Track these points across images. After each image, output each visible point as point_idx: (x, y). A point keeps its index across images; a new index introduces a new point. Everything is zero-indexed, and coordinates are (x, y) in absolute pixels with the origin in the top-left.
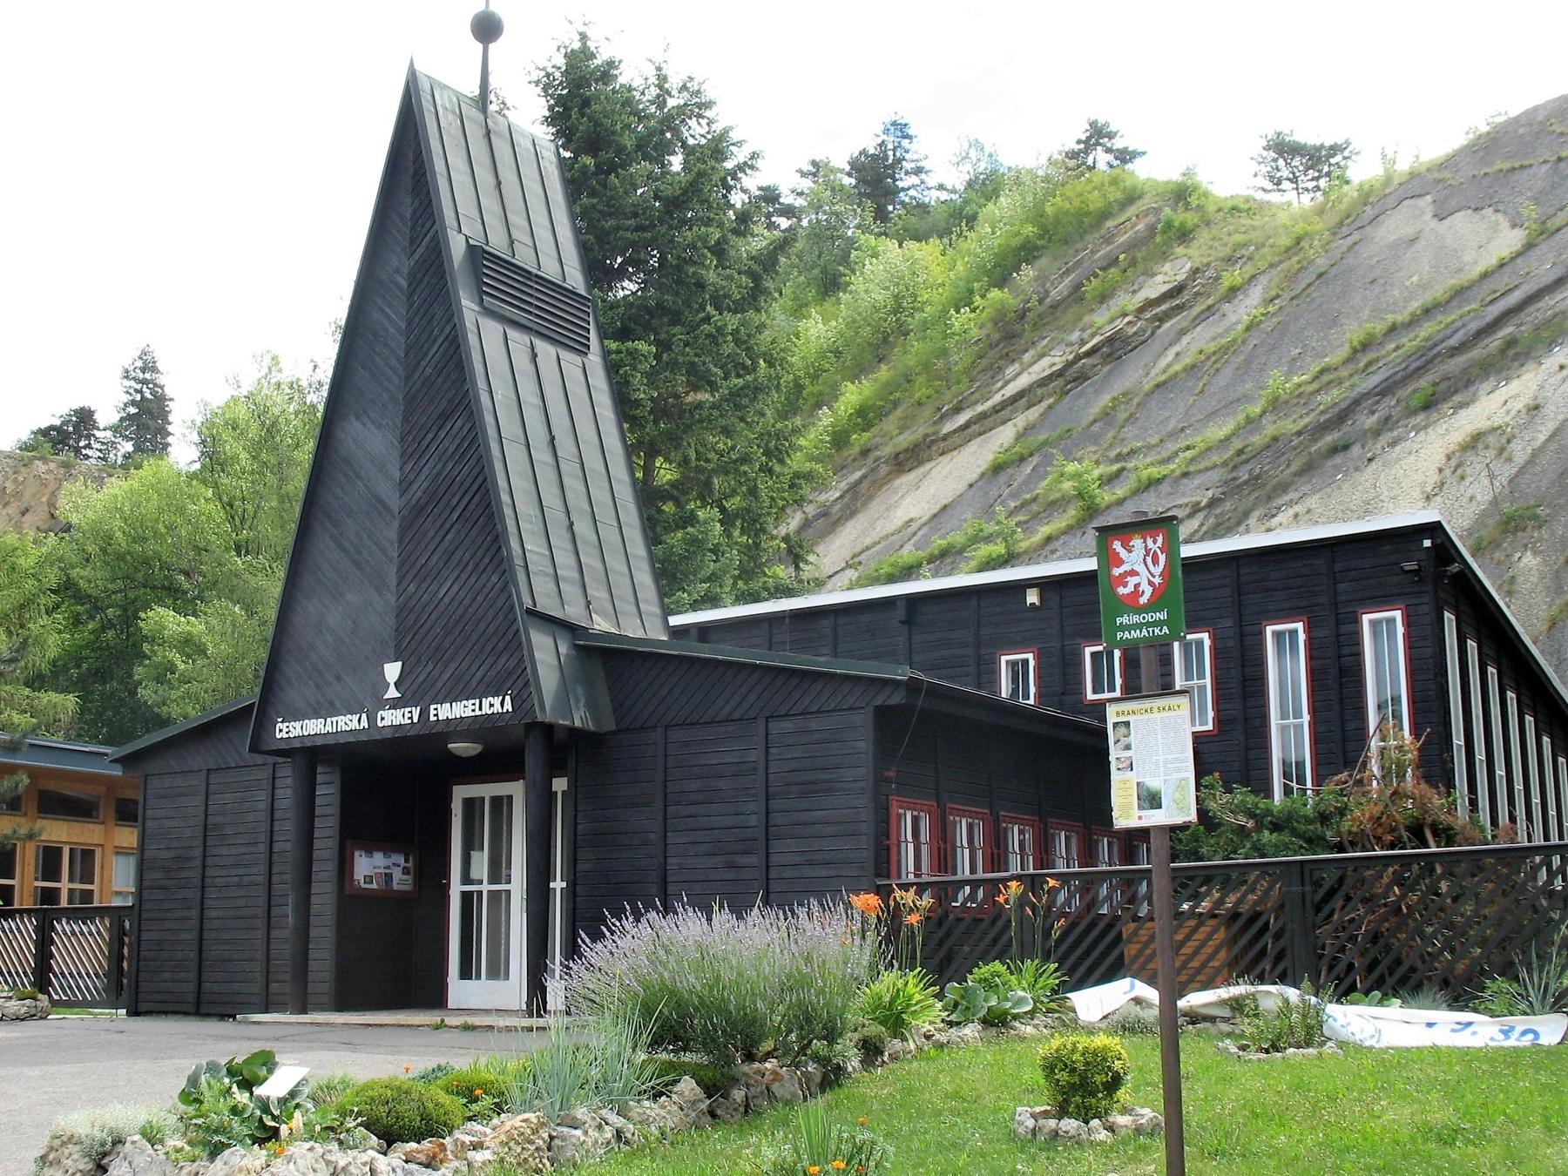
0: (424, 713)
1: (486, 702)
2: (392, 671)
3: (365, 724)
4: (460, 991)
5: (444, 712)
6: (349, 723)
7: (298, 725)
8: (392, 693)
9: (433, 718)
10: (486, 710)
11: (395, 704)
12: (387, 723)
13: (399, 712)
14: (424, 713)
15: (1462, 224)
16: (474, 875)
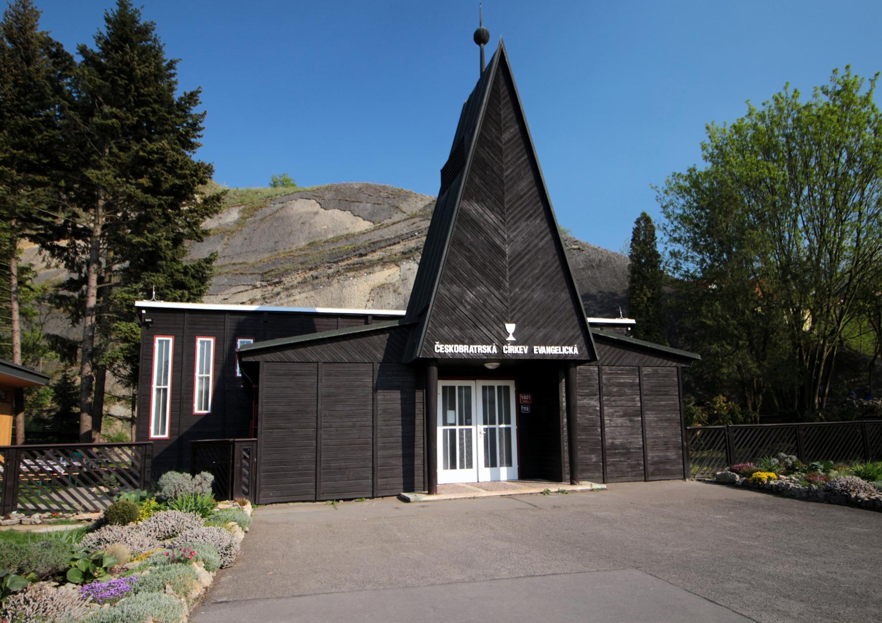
0: (531, 350)
1: (564, 348)
2: (511, 328)
3: (495, 350)
4: (444, 475)
5: (542, 350)
8: (511, 338)
9: (535, 352)
10: (564, 352)
11: (514, 343)
12: (510, 351)
13: (516, 348)
14: (531, 350)
15: (337, 213)
16: (450, 419)
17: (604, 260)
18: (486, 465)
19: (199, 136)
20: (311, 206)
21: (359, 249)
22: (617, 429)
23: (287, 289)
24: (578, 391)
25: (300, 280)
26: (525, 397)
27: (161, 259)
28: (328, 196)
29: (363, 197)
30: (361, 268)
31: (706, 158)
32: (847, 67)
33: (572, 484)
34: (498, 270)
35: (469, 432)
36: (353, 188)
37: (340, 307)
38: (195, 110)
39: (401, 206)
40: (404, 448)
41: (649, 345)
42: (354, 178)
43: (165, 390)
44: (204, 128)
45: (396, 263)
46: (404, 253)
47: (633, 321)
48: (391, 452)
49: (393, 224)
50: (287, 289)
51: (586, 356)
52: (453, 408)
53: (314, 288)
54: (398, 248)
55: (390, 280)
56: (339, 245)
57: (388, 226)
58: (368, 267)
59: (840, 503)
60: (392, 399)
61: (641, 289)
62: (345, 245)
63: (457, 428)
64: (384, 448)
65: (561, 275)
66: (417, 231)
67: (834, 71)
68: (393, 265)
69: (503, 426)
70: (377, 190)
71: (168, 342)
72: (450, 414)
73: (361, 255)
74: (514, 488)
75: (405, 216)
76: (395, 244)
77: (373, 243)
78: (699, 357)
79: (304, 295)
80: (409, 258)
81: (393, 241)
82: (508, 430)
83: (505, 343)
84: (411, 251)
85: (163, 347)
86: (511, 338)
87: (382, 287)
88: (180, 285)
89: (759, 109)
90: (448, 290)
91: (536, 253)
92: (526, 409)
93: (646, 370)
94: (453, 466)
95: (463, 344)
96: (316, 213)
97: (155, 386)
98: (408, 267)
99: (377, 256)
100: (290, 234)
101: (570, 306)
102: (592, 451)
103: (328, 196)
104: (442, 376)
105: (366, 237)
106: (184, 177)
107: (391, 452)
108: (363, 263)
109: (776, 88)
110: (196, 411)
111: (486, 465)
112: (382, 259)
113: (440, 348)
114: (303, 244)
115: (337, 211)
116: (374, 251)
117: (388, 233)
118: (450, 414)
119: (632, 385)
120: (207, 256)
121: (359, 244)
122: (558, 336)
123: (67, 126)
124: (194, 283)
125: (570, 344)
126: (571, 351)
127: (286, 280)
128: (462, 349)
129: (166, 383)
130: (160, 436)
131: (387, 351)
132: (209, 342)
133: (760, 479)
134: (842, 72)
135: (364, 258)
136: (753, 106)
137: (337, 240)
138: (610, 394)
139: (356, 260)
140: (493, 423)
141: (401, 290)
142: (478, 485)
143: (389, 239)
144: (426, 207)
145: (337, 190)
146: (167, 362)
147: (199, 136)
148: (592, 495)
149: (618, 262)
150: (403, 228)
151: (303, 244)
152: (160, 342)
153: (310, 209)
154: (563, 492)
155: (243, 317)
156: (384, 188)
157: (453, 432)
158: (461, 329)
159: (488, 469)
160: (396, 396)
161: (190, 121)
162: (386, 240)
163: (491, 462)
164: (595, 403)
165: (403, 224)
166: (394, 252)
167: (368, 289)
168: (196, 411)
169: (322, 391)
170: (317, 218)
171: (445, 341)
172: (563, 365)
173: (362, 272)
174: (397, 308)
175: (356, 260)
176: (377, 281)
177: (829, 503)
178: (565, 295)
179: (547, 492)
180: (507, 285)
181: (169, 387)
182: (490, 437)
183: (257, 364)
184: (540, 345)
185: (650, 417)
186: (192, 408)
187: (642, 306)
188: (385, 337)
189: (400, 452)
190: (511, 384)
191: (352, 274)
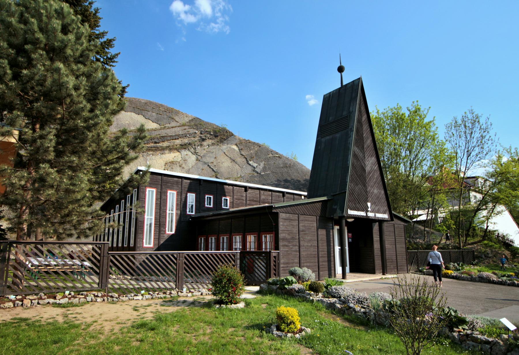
0: (375, 215)
3: (365, 215)
6: (362, 214)
11: (371, 212)
14: (375, 215)
17: (292, 164)
19: (113, 66)
21: (154, 139)
26: (350, 235)
29: (149, 108)
32: (417, 101)
33: (383, 274)
36: (141, 102)
39: (175, 118)
44: (116, 62)
45: (178, 150)
46: (181, 145)
49: (173, 127)
54: (178, 142)
55: (176, 159)
57: (169, 128)
58: (160, 150)
64: (322, 257)
65: (381, 183)
66: (189, 134)
67: (413, 102)
68: (175, 151)
71: (153, 191)
73: (156, 143)
75: (178, 124)
76: (176, 139)
77: (163, 137)
80: (185, 149)
81: (174, 138)
84: (186, 145)
85: (151, 194)
86: (369, 209)
87: (172, 163)
92: (350, 240)
98: (185, 153)
99: (165, 144)
105: (157, 133)
109: (393, 105)
110: (167, 232)
112: (169, 146)
113: (351, 212)
115: (133, 114)
116: (164, 142)
121: (153, 136)
122: (382, 209)
125: (384, 213)
130: (148, 246)
132: (173, 194)
134: (415, 103)
135: (158, 144)
141: (184, 166)
143: (172, 136)
144: (190, 121)
147: (113, 66)
149: (299, 166)
150: (179, 131)
151: (115, 130)
152: (170, 193)
161: (109, 56)
162: (170, 136)
165: (178, 129)
166: (175, 143)
167: (163, 164)
169: (301, 228)
171: (351, 209)
172: (381, 222)
173: (158, 152)
176: (168, 159)
177: (481, 282)
178: (383, 192)
183: (277, 213)
186: (165, 231)
191: (151, 153)
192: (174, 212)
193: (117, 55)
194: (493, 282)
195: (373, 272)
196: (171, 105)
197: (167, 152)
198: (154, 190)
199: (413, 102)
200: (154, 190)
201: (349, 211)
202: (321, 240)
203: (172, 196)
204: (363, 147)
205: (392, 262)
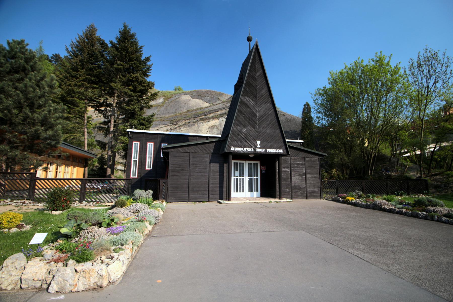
0: (266, 151)
1: (278, 150)
2: (259, 142)
3: (253, 150)
4: (234, 194)
5: (269, 151)
7: (237, 148)
8: (259, 146)
10: (278, 151)
11: (260, 148)
14: (266, 151)
15: (197, 100)
16: (236, 175)
17: (292, 119)
18: (249, 191)
20: (188, 97)
21: (205, 113)
22: (296, 180)
23: (179, 127)
24: (282, 166)
25: (184, 123)
27: (136, 115)
28: (194, 94)
29: (206, 94)
30: (205, 120)
31: (329, 83)
32: (381, 52)
33: (280, 199)
34: (254, 122)
35: (243, 179)
37: (198, 133)
38: (149, 63)
40: (220, 184)
41: (308, 150)
42: (204, 89)
43: (136, 161)
45: (218, 118)
47: (302, 141)
48: (215, 185)
50: (179, 127)
51: (285, 153)
52: (237, 170)
53: (189, 126)
54: (219, 113)
55: (215, 124)
56: (198, 111)
57: (215, 105)
58: (208, 120)
59: (378, 210)
60: (216, 167)
61: (306, 130)
62: (199, 112)
63: (239, 177)
64: (213, 184)
69: (255, 177)
70: (211, 92)
71: (137, 144)
72: (236, 172)
73: (205, 115)
74: (259, 200)
75: (221, 102)
78: (327, 155)
79: (185, 129)
82: (257, 179)
83: (257, 147)
85: (136, 146)
86: (259, 146)
87: (213, 126)
88: (142, 124)
89: (349, 66)
90: (236, 128)
91: (268, 116)
93: (307, 159)
94: (237, 191)
95: (242, 147)
96: (190, 100)
97: (133, 159)
100: (181, 107)
101: (280, 135)
102: (287, 188)
103: (194, 94)
104: (234, 159)
105: (207, 109)
106: (145, 86)
107: (215, 185)
108: (206, 118)
109: (356, 59)
110: (147, 168)
111: (249, 191)
113: (233, 149)
114: (185, 111)
115: (197, 99)
117: (215, 108)
118: (236, 172)
119: (302, 164)
120: (152, 114)
121: (205, 111)
122: (275, 146)
123: (105, 68)
124: (147, 123)
126: (280, 151)
127: (179, 123)
128: (241, 149)
129: (136, 158)
131: (214, 149)
133: (349, 200)
134: (379, 54)
136: (347, 65)
137: (197, 109)
138: (294, 167)
139: (204, 117)
140: (252, 176)
141: (219, 128)
142: (246, 198)
144: (228, 99)
145: (197, 92)
146: (137, 151)
148: (287, 204)
149: (297, 120)
150: (220, 106)
152: (135, 144)
153: (188, 98)
154: (276, 202)
155: (164, 136)
156: (214, 91)
157: (237, 179)
158: (241, 142)
159: (250, 193)
160: (217, 165)
163: (251, 190)
164: (288, 170)
165: (220, 105)
168: (147, 168)
169: (191, 163)
170: (190, 102)
171: (235, 146)
172: (277, 156)
174: (218, 134)
175: (204, 117)
178: (278, 131)
179: (271, 202)
180: (257, 127)
181: (137, 160)
182: (250, 181)
184: (269, 149)
185: (308, 176)
186: (145, 167)
187: (306, 136)
188: (214, 144)
189: (218, 186)
190: (258, 163)
192: (152, 156)
193: (151, 65)
194: (384, 210)
195: (274, 197)
196: (219, 91)
197: (211, 120)
198: (139, 143)
199: (376, 53)
200: (139, 143)
201: (232, 148)
202: (213, 171)
203: (150, 146)
204: (256, 97)
205: (299, 189)
